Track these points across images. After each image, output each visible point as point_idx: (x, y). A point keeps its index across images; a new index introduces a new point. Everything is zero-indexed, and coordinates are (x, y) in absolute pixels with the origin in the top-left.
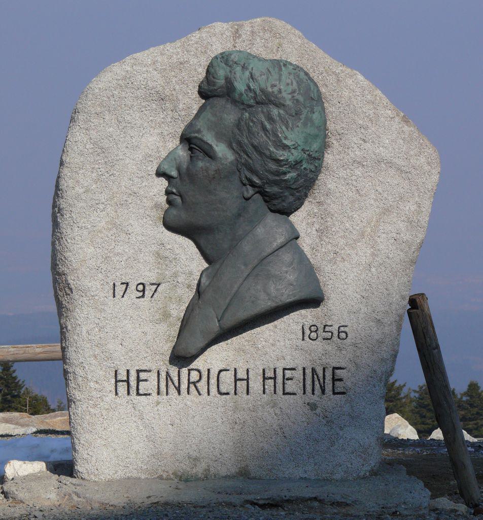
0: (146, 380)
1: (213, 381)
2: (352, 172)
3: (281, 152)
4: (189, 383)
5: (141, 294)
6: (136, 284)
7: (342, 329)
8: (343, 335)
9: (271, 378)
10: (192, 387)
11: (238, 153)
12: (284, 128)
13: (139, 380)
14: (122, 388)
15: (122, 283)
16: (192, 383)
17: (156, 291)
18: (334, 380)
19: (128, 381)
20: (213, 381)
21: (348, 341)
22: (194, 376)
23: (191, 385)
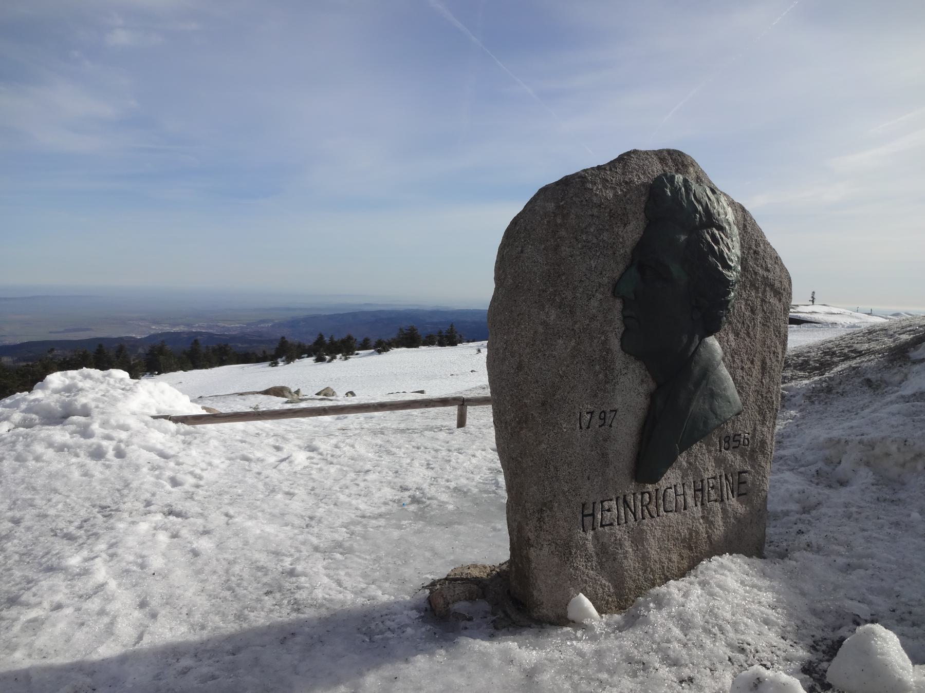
0: (609, 510)
1: (661, 501)
4: (642, 506)
18: (740, 483)
19: (593, 515)
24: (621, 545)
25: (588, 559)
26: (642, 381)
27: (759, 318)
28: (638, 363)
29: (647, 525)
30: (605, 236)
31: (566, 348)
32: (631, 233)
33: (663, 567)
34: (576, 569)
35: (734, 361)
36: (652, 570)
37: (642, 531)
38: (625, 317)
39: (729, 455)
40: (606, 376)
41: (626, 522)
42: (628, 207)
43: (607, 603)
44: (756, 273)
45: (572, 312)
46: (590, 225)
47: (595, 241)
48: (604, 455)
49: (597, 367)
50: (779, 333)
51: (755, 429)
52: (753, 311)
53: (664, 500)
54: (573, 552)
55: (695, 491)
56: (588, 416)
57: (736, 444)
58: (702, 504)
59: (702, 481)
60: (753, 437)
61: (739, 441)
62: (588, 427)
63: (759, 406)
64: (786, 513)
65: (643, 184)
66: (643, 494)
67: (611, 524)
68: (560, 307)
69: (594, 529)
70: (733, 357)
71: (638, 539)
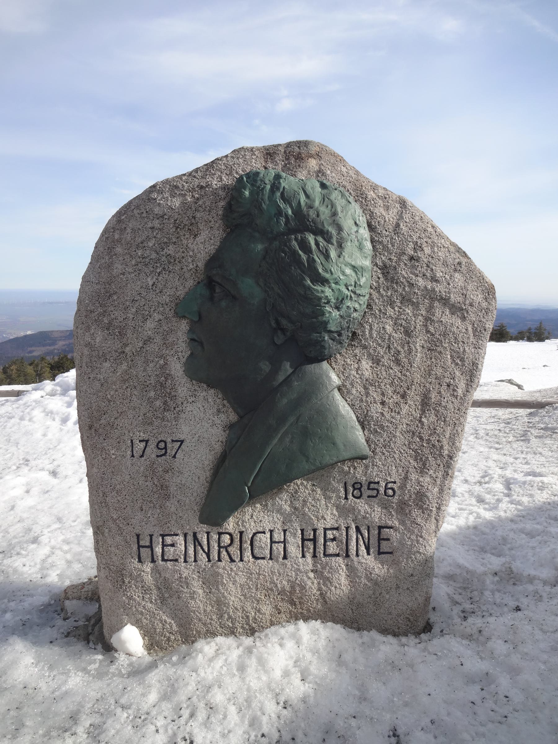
0: (173, 545)
1: (247, 545)
2: (401, 310)
3: (319, 288)
4: (219, 546)
5: (164, 451)
6: (157, 441)
7: (390, 485)
8: (390, 492)
9: (309, 540)
10: (224, 553)
11: (266, 291)
12: (322, 257)
13: (164, 545)
14: (145, 552)
15: (140, 441)
16: (222, 547)
17: (179, 447)
18: (380, 539)
19: (151, 547)
20: (247, 545)
21: (396, 499)
22: (226, 539)
23: (222, 550)
24: (187, 584)
25: (146, 590)
26: (219, 411)
27: (420, 341)
28: (212, 391)
29: (224, 569)
30: (171, 251)
31: (115, 371)
32: (204, 243)
33: (248, 617)
34: (131, 598)
35: (367, 394)
36: (230, 617)
37: (218, 574)
38: (192, 340)
39: (362, 506)
40: (165, 403)
41: (195, 561)
42: (198, 215)
43: (169, 639)
44: (411, 285)
45: (122, 334)
46: (148, 238)
47: (154, 256)
48: (164, 487)
49: (152, 394)
50: (462, 360)
51: (406, 478)
52: (408, 333)
53: (252, 544)
54: (127, 581)
55: (303, 540)
56: (142, 445)
57: (374, 493)
58: (314, 556)
59: (315, 530)
60: (403, 487)
61: (378, 491)
62: (142, 456)
63: (415, 451)
64: (531, 580)
65: (224, 188)
66: (220, 534)
67: (176, 560)
68: (108, 329)
69: (153, 561)
70: (365, 388)
71: (211, 582)
